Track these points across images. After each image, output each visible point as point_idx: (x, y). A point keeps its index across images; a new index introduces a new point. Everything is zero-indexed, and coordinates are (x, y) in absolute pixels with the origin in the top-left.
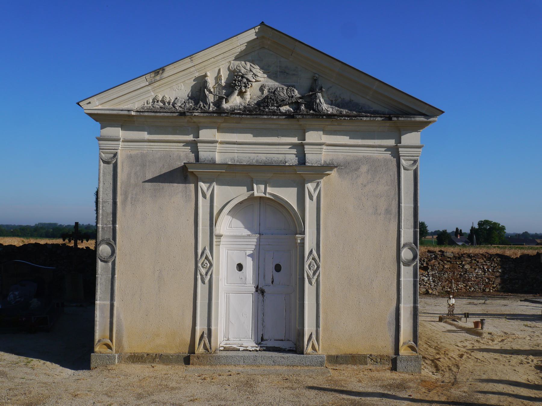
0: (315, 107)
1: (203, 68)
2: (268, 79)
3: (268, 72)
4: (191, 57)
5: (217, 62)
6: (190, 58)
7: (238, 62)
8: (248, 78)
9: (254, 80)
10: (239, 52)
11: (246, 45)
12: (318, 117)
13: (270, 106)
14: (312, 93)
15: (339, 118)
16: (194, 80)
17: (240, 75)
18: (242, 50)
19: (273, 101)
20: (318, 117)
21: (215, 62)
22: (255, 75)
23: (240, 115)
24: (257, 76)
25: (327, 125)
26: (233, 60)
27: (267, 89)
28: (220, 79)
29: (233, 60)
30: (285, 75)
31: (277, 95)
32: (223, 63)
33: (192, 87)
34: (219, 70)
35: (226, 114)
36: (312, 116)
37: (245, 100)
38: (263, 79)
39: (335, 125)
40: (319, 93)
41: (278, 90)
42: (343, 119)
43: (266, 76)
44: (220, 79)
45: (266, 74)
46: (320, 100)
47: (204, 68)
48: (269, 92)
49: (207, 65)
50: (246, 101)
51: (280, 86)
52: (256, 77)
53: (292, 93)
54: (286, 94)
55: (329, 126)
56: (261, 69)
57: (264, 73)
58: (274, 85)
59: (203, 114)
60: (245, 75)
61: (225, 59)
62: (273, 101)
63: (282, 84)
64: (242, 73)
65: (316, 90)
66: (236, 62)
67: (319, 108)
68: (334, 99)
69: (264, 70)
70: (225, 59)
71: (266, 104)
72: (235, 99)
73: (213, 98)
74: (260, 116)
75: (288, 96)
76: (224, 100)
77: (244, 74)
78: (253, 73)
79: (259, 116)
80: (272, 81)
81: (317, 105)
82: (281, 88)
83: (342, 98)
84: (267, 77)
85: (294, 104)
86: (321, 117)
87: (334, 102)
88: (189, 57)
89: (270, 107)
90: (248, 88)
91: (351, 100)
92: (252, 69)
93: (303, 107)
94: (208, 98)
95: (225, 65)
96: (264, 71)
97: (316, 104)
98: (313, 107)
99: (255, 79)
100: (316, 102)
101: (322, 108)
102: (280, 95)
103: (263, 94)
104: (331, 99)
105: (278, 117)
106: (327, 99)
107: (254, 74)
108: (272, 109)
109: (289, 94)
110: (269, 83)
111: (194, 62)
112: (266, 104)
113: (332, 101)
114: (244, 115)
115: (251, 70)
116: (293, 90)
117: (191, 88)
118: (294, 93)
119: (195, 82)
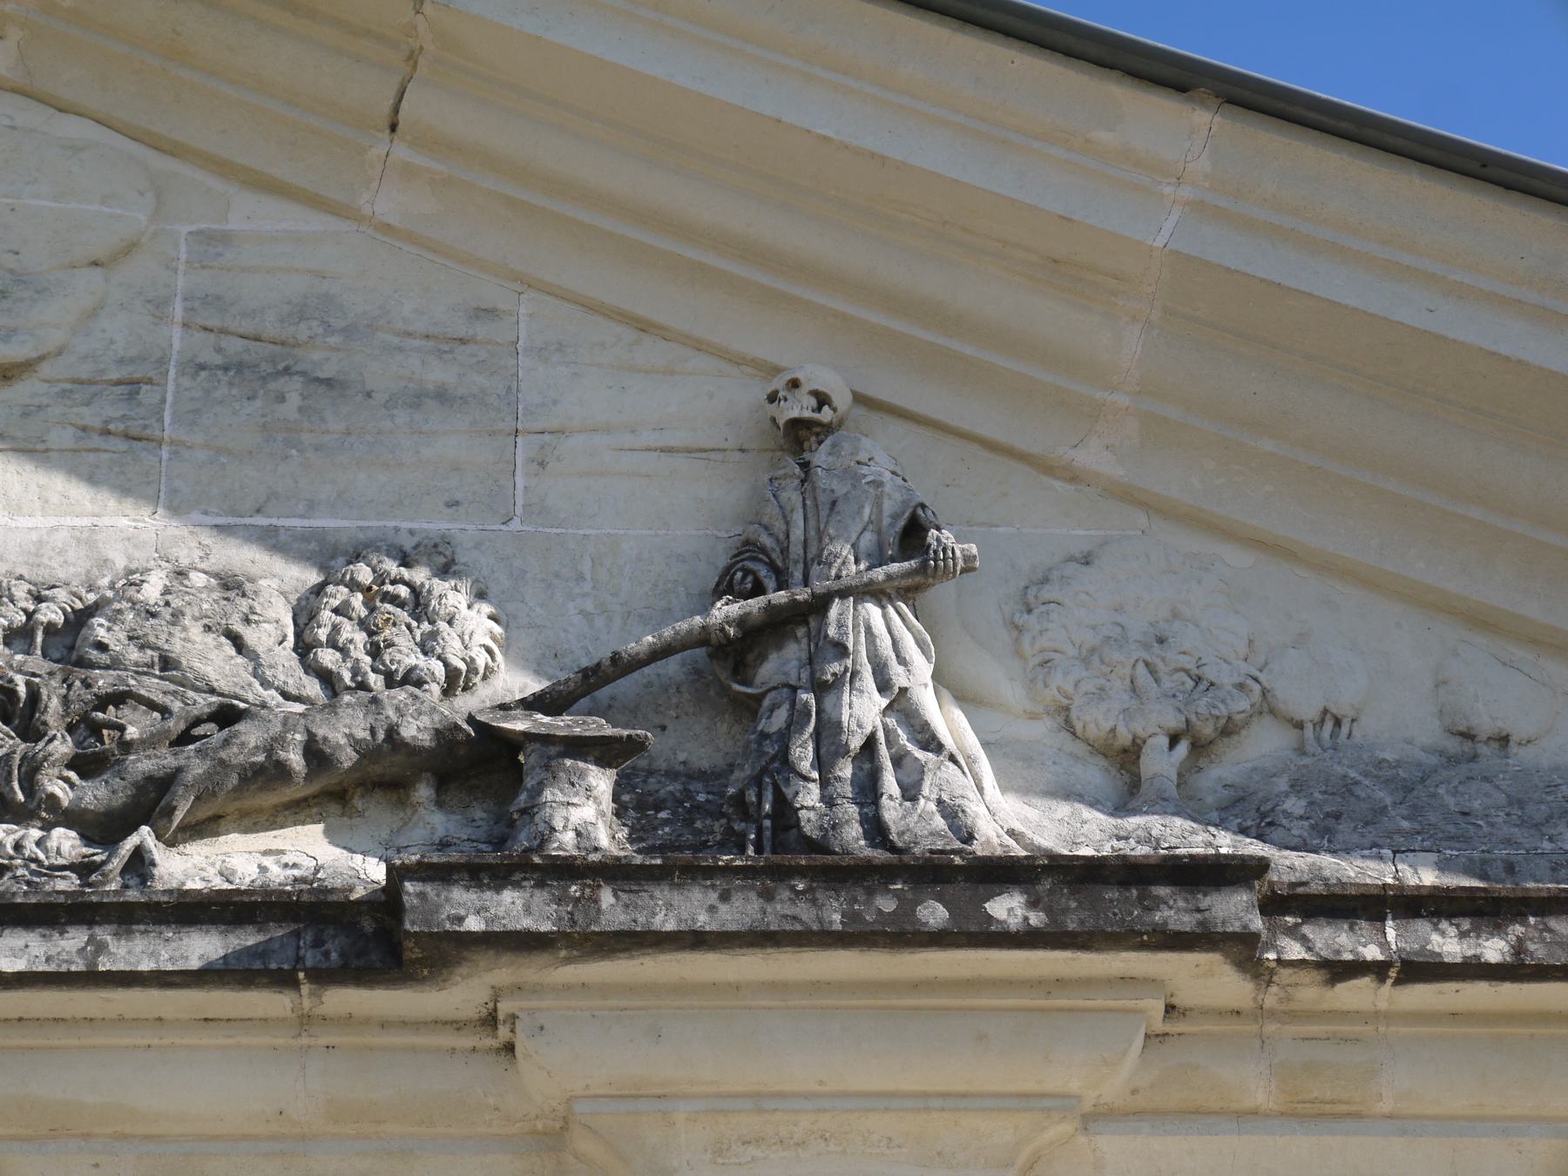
0: (809, 797)
12: (887, 905)
14: (755, 604)
15: (1292, 932)
20: (887, 905)
25: (1096, 1118)
30: (281, 398)
31: (116, 664)
36: (768, 896)
39: (1247, 1117)
40: (872, 611)
41: (151, 592)
42: (1372, 953)
46: (900, 704)
51: (186, 554)
53: (404, 641)
54: (285, 657)
55: (1111, 1145)
58: (87, 539)
63: (222, 529)
65: (814, 558)
67: (892, 810)
68: (1174, 721)
75: (327, 678)
80: (59, 486)
81: (846, 770)
82: (198, 579)
83: (1309, 713)
85: (424, 792)
86: (934, 914)
87: (1160, 763)
91: (1468, 736)
93: (584, 813)
97: (823, 763)
98: (785, 811)
100: (829, 737)
101: (950, 812)
104: (1098, 720)
106: (1041, 731)
109: (343, 651)
113: (1126, 757)
116: (419, 605)
118: (434, 635)
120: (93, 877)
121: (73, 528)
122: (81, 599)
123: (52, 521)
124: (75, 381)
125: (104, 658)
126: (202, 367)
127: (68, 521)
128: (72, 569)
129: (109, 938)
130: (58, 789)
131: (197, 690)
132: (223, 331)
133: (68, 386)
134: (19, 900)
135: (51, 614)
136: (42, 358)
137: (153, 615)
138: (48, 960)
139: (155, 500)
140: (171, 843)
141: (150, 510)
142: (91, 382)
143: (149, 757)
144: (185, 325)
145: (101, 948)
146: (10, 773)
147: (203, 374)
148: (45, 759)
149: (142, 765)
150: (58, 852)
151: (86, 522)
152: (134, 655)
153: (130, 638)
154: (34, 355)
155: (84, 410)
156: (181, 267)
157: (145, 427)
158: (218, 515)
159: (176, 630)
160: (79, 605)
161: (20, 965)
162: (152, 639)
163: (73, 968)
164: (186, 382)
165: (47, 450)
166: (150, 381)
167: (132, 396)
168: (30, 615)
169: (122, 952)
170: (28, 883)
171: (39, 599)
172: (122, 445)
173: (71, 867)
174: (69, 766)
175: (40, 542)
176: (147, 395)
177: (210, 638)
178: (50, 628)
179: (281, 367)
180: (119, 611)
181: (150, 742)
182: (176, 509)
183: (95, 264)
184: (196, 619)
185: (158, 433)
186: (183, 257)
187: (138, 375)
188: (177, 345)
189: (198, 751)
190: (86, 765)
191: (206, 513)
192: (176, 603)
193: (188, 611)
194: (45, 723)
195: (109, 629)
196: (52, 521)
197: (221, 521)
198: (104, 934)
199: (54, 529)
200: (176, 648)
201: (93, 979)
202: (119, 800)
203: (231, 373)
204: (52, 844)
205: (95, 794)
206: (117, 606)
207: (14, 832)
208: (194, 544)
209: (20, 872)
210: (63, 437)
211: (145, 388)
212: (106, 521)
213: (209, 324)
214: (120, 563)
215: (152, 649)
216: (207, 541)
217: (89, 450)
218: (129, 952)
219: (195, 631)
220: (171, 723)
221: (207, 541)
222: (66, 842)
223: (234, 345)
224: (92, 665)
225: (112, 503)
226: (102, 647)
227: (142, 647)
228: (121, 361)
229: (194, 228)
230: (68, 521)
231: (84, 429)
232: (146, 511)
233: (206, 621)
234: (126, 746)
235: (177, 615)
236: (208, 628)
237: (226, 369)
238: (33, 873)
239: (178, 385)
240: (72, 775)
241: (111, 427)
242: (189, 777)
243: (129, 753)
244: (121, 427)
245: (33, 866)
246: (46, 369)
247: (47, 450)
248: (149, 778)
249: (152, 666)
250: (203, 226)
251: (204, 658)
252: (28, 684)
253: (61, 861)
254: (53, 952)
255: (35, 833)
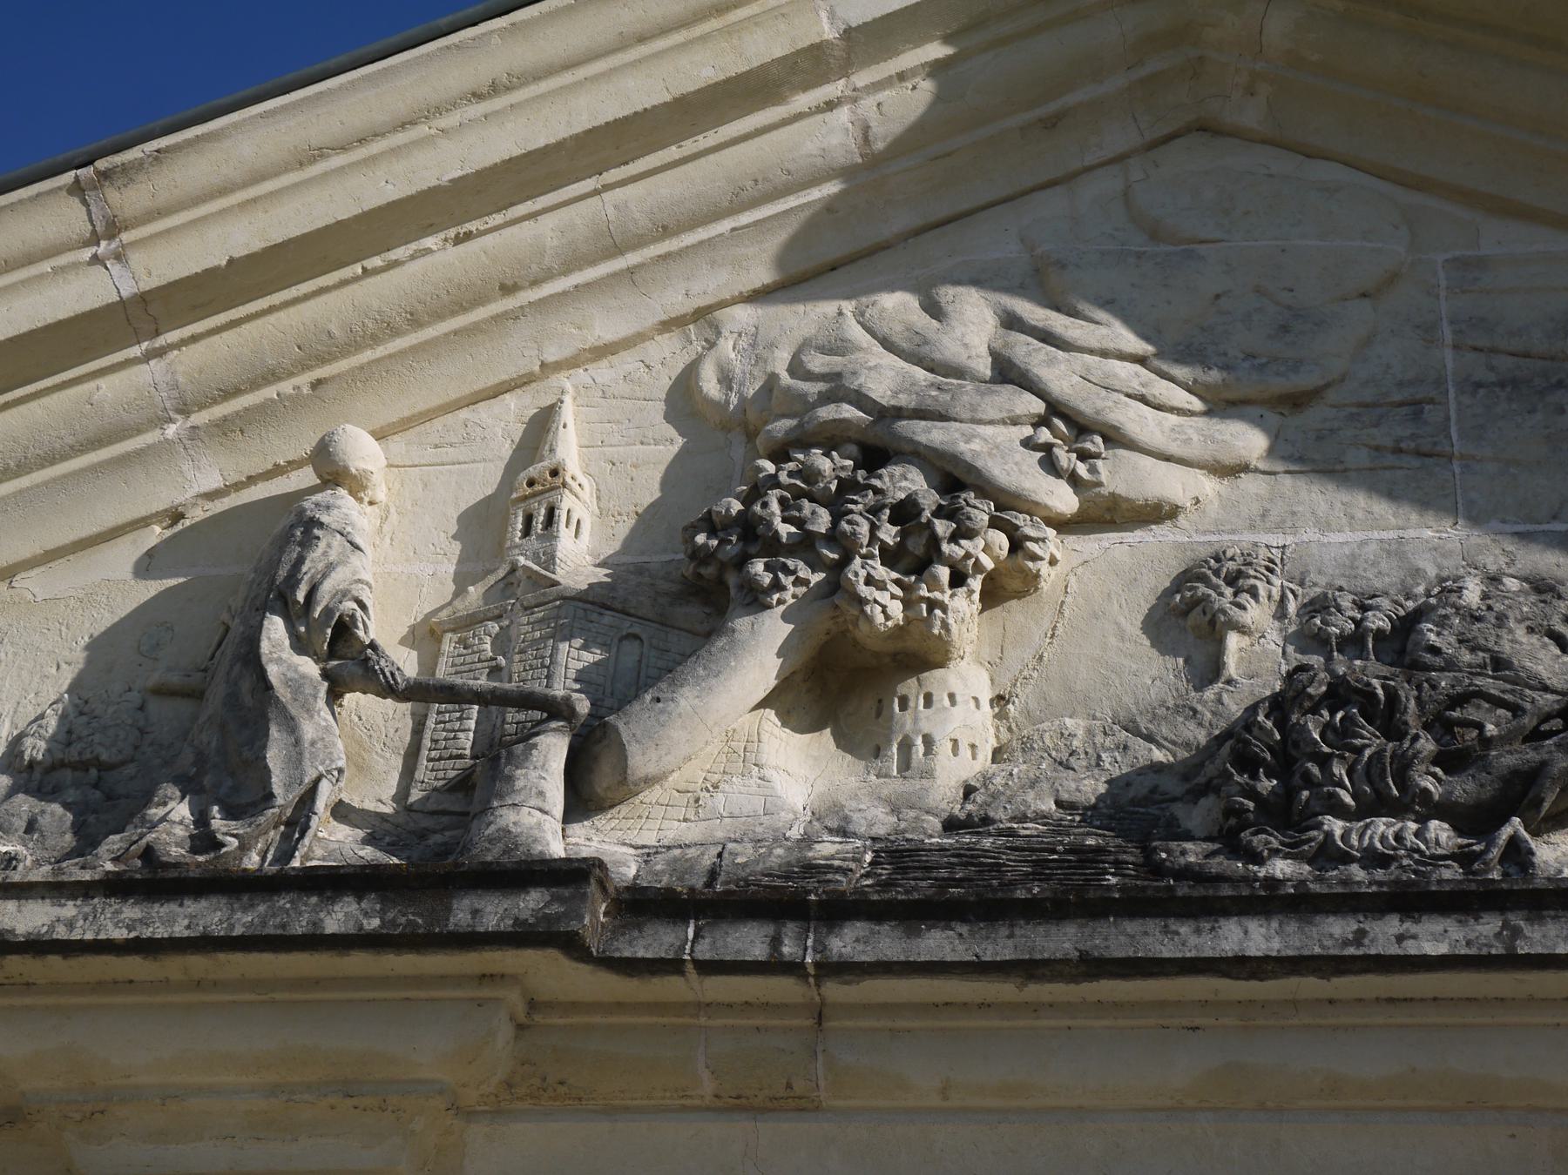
1: (286, 387)
2: (1287, 481)
3: (1280, 384)
4: (102, 164)
5: (510, 303)
6: (77, 189)
7: (829, 308)
8: (955, 459)
9: (1065, 500)
10: (846, 173)
11: (936, 69)
13: (1340, 811)
16: (147, 566)
17: (831, 439)
18: (880, 146)
19: (1392, 727)
21: (479, 300)
22: (1081, 427)
23: (791, 929)
24: (1115, 438)
26: (758, 296)
27: (1281, 614)
28: (529, 520)
29: (758, 296)
31: (1450, 665)
32: (605, 326)
33: (96, 647)
34: (542, 426)
35: (532, 902)
37: (905, 764)
38: (1208, 486)
41: (1472, 594)
43: (1249, 441)
44: (529, 520)
45: (1258, 422)
47: (304, 380)
48: (1310, 639)
49: (353, 345)
50: (928, 774)
51: (1493, 561)
52: (1084, 456)
56: (1181, 359)
57: (1220, 405)
58: (1396, 550)
59: (131, 911)
60: (921, 414)
61: (631, 271)
62: (1392, 727)
63: (1524, 537)
64: (860, 399)
66: (800, 308)
69: (1226, 367)
70: (632, 258)
71: (1266, 785)
72: (746, 757)
73: (397, 763)
74: (1153, 925)
76: (553, 749)
77: (898, 413)
78: (1038, 406)
79: (1132, 926)
80: (1360, 501)
82: (1512, 584)
84: (1271, 452)
88: (68, 178)
89: (1336, 826)
90: (958, 580)
92: (1028, 353)
94: (291, 726)
95: (627, 362)
96: (1214, 376)
99: (1074, 480)
102: (1499, 664)
103: (1209, 670)
105: (1488, 928)
107: (1055, 409)
108: (1374, 859)
110: (1310, 534)
111: (135, 258)
112: (1266, 785)
114: (858, 928)
115: (1007, 372)
117: (79, 657)
119: (152, 588)
120: (1476, 866)
121: (1381, 541)
122: (1402, 606)
123: (1360, 536)
124: (1360, 405)
125: (1438, 661)
126: (1479, 385)
127: (1376, 535)
128: (1387, 579)
129: (1522, 923)
130: (1428, 783)
131: (1531, 688)
132: (1493, 351)
133: (1354, 410)
134: (1434, 888)
135: (1377, 621)
136: (1328, 386)
137: (1479, 619)
138: (1469, 943)
139: (1453, 512)
140: (1536, 834)
141: (1450, 522)
142: (1374, 405)
143: (1510, 752)
144: (1456, 347)
145: (1516, 933)
146: (1384, 770)
147: (1482, 392)
148: (1415, 756)
149: (1508, 759)
150: (1437, 843)
151: (1392, 534)
152: (1466, 657)
153: (1460, 642)
154: (1321, 383)
155: (1375, 431)
156: (1443, 294)
157: (1435, 444)
158: (1515, 523)
159: (1503, 632)
160: (1402, 613)
161: (1443, 949)
162: (1482, 642)
163: (1494, 952)
164: (1466, 400)
165: (1346, 470)
166: (1431, 401)
167: (1417, 416)
168: (1358, 623)
169: (1537, 936)
170: (1415, 872)
171: (1364, 608)
172: (1416, 463)
173: (1452, 857)
174: (1435, 763)
175: (1353, 557)
176: (1432, 414)
177: (1534, 639)
178: (1379, 633)
179: (1554, 380)
180: (1446, 617)
181: (1505, 739)
182: (1476, 519)
183: (1364, 295)
184: (1519, 622)
185: (1448, 449)
186: (1443, 283)
187: (1419, 396)
188: (1450, 365)
189: (1558, 746)
190: (1450, 761)
191: (1504, 521)
192: (1498, 607)
193: (1510, 613)
194: (1406, 723)
195: (1438, 634)
196: (1360, 536)
197: (1520, 528)
198: (1517, 919)
199: (1363, 543)
200: (1506, 648)
201: (1512, 961)
202: (1488, 792)
203: (1509, 389)
204: (1431, 835)
205: (1463, 788)
206: (1442, 612)
207: (1393, 825)
208: (1498, 551)
209: (1405, 862)
210: (1359, 457)
211: (1427, 407)
212: (1411, 533)
213: (1480, 343)
214: (1432, 572)
215: (1483, 651)
216: (1510, 548)
217: (1385, 468)
218: (1544, 936)
219: (1520, 633)
220: (1526, 720)
221: (1510, 548)
222: (1439, 830)
223: (1505, 363)
224: (1428, 668)
225: (1414, 517)
226: (1436, 651)
227: (1473, 650)
228: (1400, 384)
229: (1449, 256)
230: (1376, 535)
231: (1377, 448)
232: (1448, 522)
233: (1528, 623)
234: (1486, 742)
235: (1501, 619)
236: (1531, 630)
237: (1502, 385)
238: (1417, 862)
239: (1459, 403)
240: (1438, 770)
241: (1403, 445)
242: (1555, 770)
243: (1489, 749)
244: (1413, 445)
245: (1416, 856)
246: (1332, 396)
247: (1346, 470)
248: (1515, 772)
249: (1484, 666)
250: (1457, 253)
251: (1533, 658)
252: (1384, 687)
253: (1440, 851)
254: (1472, 936)
255: (1413, 826)
